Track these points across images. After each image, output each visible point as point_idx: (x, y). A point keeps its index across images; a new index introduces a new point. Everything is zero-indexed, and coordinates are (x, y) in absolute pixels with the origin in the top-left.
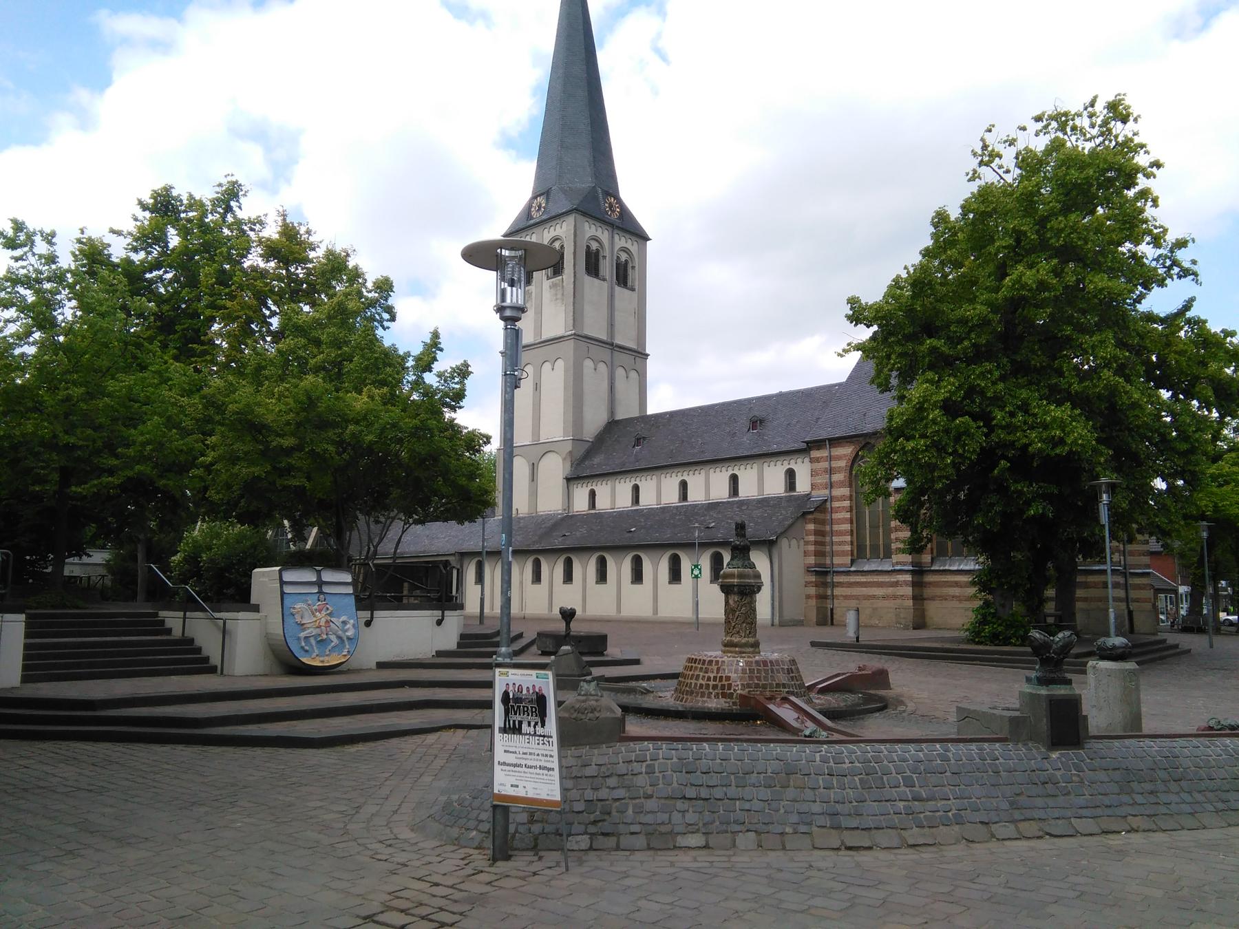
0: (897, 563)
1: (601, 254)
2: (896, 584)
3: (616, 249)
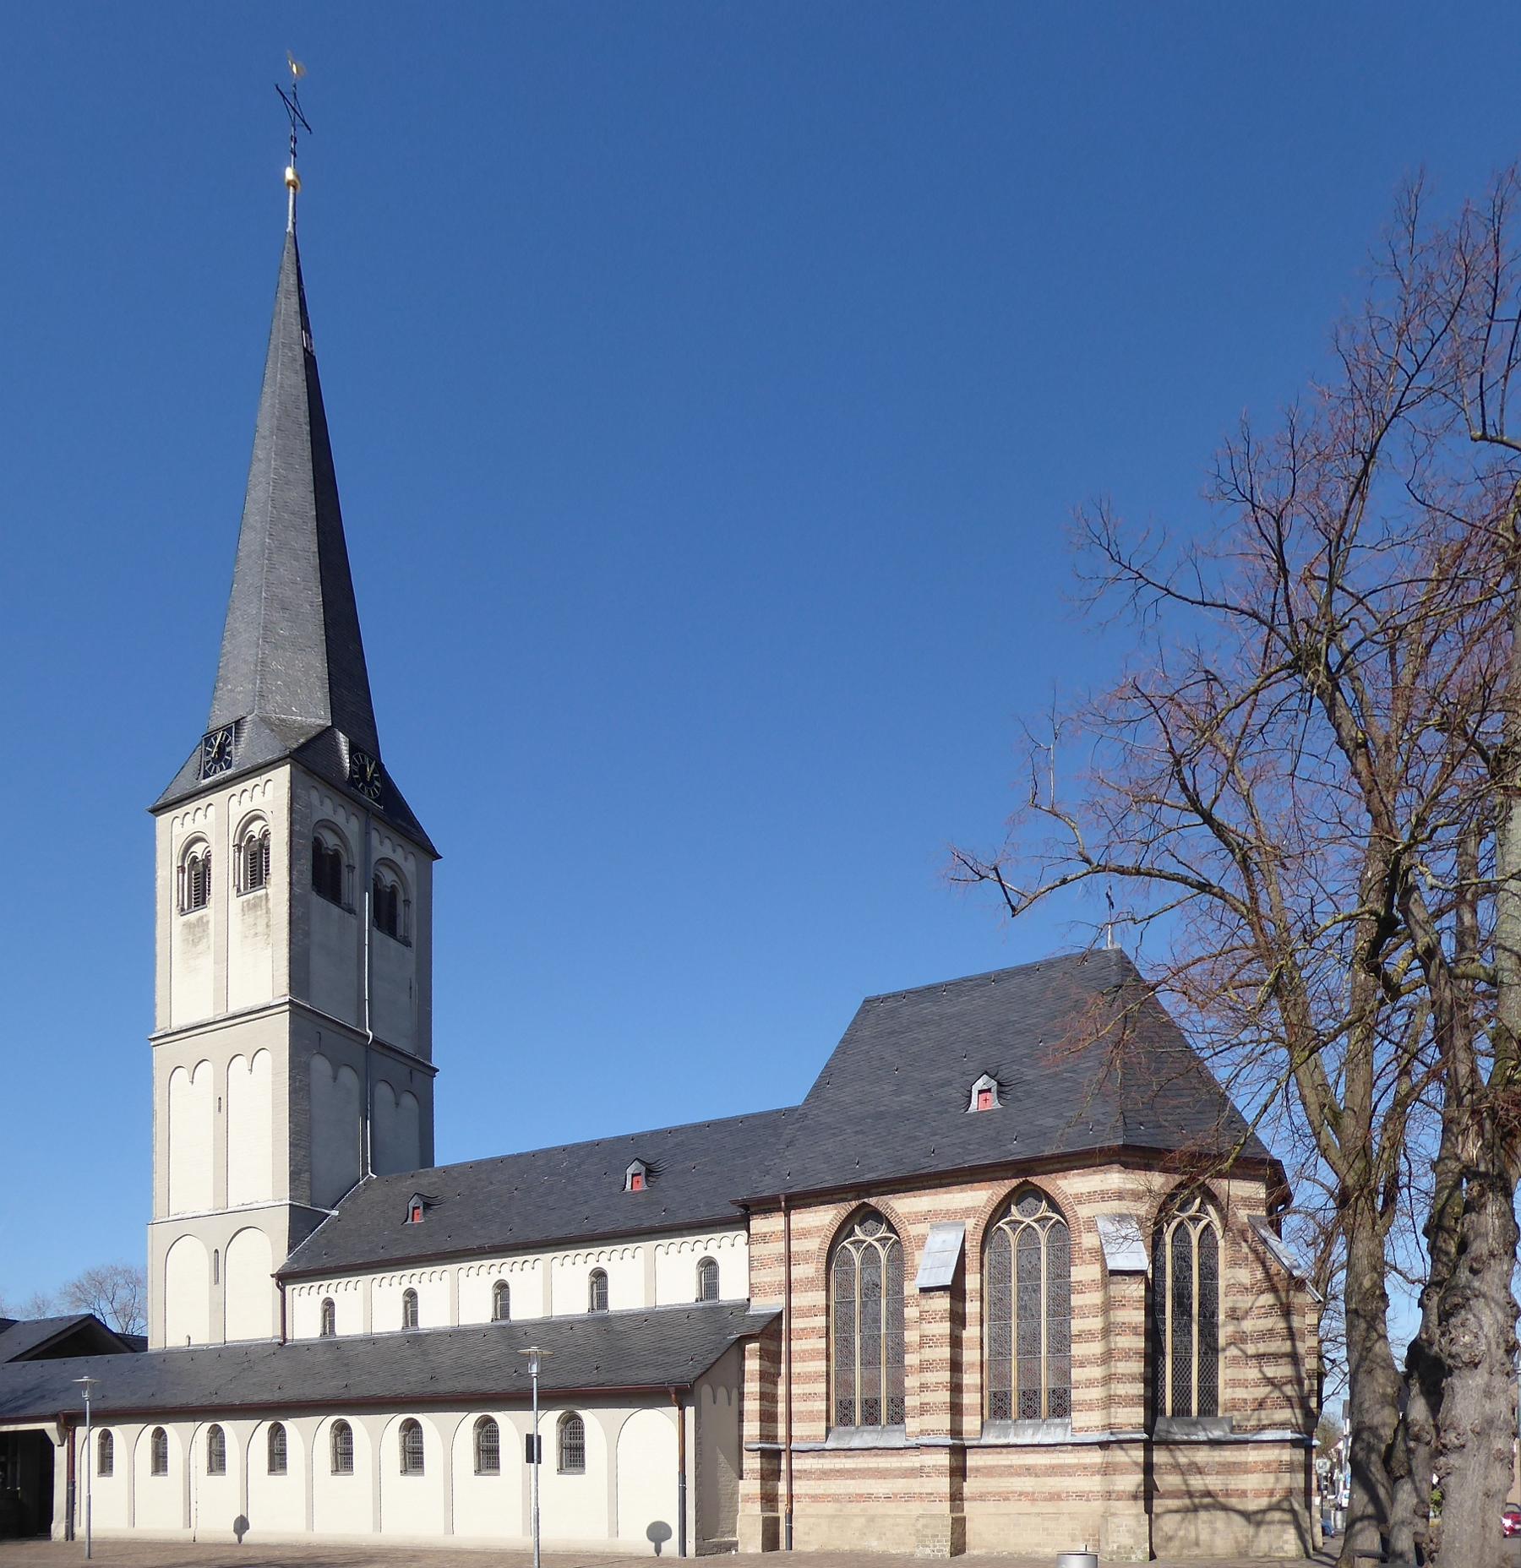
0: (922, 1432)
1: (345, 860)
2: (919, 1472)
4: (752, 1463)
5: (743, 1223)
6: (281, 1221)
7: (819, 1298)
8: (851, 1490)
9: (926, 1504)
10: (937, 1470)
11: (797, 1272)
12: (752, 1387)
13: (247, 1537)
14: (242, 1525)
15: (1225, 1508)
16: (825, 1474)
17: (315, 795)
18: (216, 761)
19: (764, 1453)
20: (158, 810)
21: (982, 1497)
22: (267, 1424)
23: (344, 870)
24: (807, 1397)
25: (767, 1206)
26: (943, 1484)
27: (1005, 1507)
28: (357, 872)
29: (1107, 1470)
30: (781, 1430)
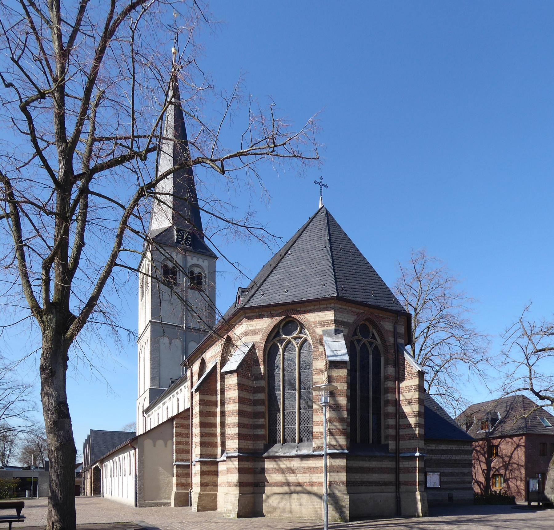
15: (309, 493)
19: (178, 466)
29: (331, 470)
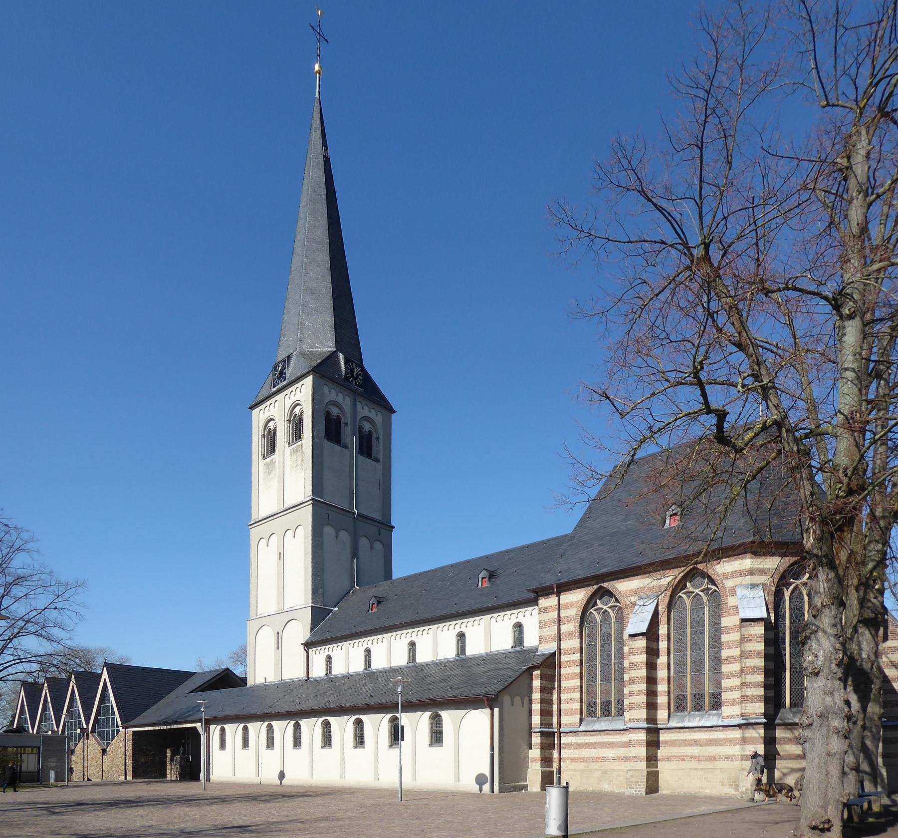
0: (630, 720)
1: (343, 421)
2: (629, 744)
3: (359, 417)
4: (536, 739)
5: (534, 602)
6: (308, 615)
7: (576, 643)
8: (593, 755)
9: (632, 763)
10: (639, 743)
11: (563, 628)
12: (536, 696)
13: (284, 782)
14: (282, 775)
16: (579, 746)
17: (326, 389)
18: (279, 378)
19: (543, 734)
20: (252, 408)
21: (668, 759)
22: (293, 723)
23: (343, 425)
24: (569, 701)
25: (546, 591)
26: (642, 751)
27: (682, 765)
28: (349, 426)
30: (555, 721)
